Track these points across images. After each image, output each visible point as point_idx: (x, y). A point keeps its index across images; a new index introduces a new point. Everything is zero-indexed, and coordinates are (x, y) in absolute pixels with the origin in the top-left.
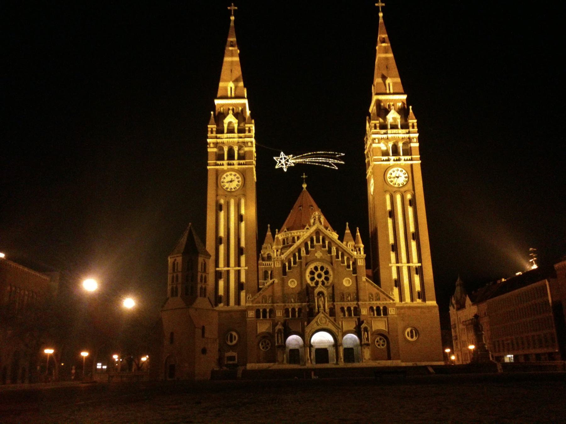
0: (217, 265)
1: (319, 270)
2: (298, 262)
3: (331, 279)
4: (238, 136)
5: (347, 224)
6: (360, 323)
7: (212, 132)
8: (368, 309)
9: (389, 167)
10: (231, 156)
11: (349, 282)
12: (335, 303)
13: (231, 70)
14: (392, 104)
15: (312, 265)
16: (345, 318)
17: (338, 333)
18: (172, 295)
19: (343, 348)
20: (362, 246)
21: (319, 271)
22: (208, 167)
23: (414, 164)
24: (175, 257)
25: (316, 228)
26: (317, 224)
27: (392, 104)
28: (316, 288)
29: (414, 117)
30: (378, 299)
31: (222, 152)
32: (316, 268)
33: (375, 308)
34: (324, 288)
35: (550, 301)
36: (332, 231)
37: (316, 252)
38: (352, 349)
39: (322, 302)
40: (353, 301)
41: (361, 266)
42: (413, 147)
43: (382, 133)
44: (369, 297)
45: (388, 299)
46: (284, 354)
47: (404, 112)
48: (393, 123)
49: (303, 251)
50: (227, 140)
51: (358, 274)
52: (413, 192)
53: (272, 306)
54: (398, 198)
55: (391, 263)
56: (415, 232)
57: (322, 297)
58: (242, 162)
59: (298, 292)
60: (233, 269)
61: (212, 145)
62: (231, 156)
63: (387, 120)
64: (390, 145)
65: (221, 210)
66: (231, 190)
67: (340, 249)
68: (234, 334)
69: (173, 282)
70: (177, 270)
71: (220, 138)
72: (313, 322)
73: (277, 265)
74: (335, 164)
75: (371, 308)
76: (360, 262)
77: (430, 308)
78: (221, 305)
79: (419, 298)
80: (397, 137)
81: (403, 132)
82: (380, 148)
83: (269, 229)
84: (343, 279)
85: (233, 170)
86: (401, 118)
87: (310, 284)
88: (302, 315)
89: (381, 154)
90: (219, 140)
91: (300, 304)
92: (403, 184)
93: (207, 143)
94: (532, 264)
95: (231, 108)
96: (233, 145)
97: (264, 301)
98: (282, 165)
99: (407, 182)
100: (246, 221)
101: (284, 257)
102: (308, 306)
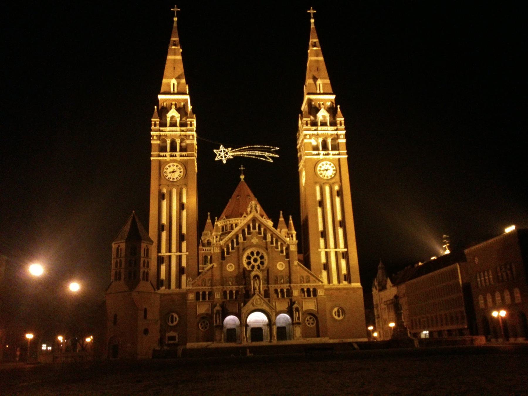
0: (159, 251)
1: (255, 255)
2: (236, 247)
3: (266, 263)
4: (180, 129)
5: (281, 212)
6: (292, 303)
7: (155, 125)
8: (300, 290)
10: (173, 148)
11: (283, 265)
12: (270, 286)
13: (174, 68)
14: (322, 103)
15: (249, 250)
16: (278, 299)
17: (272, 313)
18: (116, 280)
19: (276, 327)
20: (294, 232)
21: (255, 256)
22: (152, 158)
24: (118, 243)
25: (253, 216)
26: (254, 212)
27: (322, 103)
28: (252, 272)
29: (342, 116)
30: (308, 282)
31: (164, 144)
32: (252, 253)
33: (305, 290)
34: (259, 271)
35: (461, 283)
36: (267, 219)
37: (252, 238)
38: (284, 328)
40: (287, 283)
41: (293, 251)
42: (341, 143)
43: (313, 129)
45: (317, 281)
46: (221, 333)
47: (332, 111)
48: (322, 120)
49: (241, 238)
50: (169, 133)
51: (290, 259)
52: (340, 184)
53: (211, 289)
54: (327, 189)
55: (320, 248)
58: (184, 153)
59: (235, 275)
60: (174, 255)
61: (155, 138)
62: (173, 148)
63: (318, 118)
64: (320, 140)
65: (163, 199)
66: (173, 180)
67: (274, 235)
68: (175, 315)
69: (116, 267)
70: (121, 255)
71: (163, 131)
72: (249, 304)
73: (216, 250)
75: (302, 290)
76: (292, 247)
77: (355, 289)
78: (164, 288)
79: (345, 280)
81: (332, 129)
82: (310, 143)
83: (209, 217)
85: (175, 161)
86: (330, 116)
87: (247, 268)
88: (238, 296)
89: (312, 149)
90: (162, 133)
91: (237, 286)
93: (150, 136)
94: (445, 249)
95: (174, 103)
96: (175, 137)
97: (203, 284)
98: (222, 157)
99: (335, 174)
100: (188, 209)
101: (223, 243)
102: (245, 288)
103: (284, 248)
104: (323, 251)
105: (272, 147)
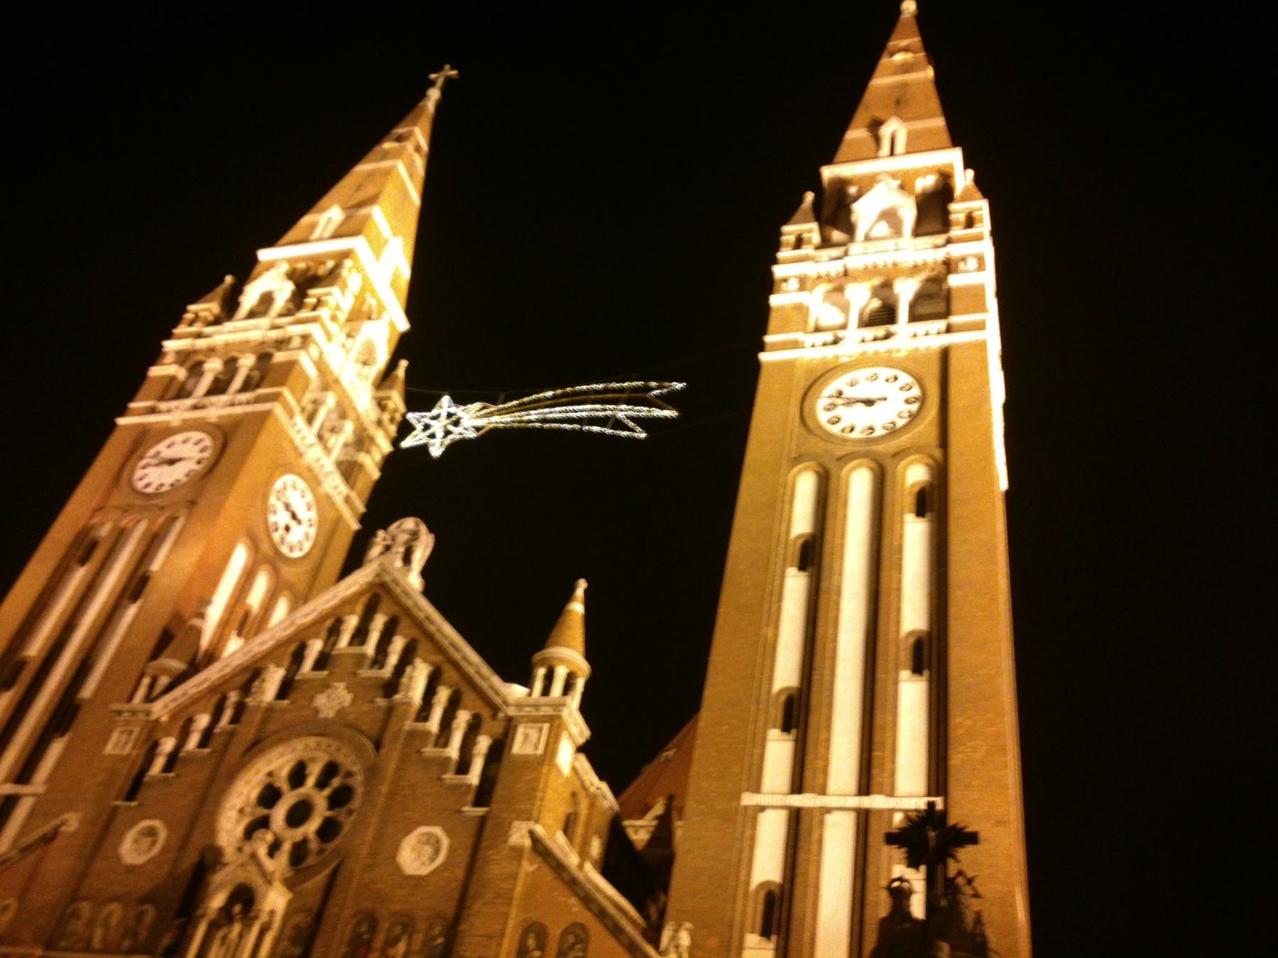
1: (311, 781)
15: (280, 749)
32: (297, 777)
37: (325, 686)
39: (223, 951)
42: (961, 289)
52: (938, 453)
64: (861, 297)
67: (449, 673)
74: (638, 420)
76: (526, 736)
84: (408, 831)
98: (432, 436)
99: (914, 417)
101: (165, 707)
103: (483, 743)
105: (653, 384)
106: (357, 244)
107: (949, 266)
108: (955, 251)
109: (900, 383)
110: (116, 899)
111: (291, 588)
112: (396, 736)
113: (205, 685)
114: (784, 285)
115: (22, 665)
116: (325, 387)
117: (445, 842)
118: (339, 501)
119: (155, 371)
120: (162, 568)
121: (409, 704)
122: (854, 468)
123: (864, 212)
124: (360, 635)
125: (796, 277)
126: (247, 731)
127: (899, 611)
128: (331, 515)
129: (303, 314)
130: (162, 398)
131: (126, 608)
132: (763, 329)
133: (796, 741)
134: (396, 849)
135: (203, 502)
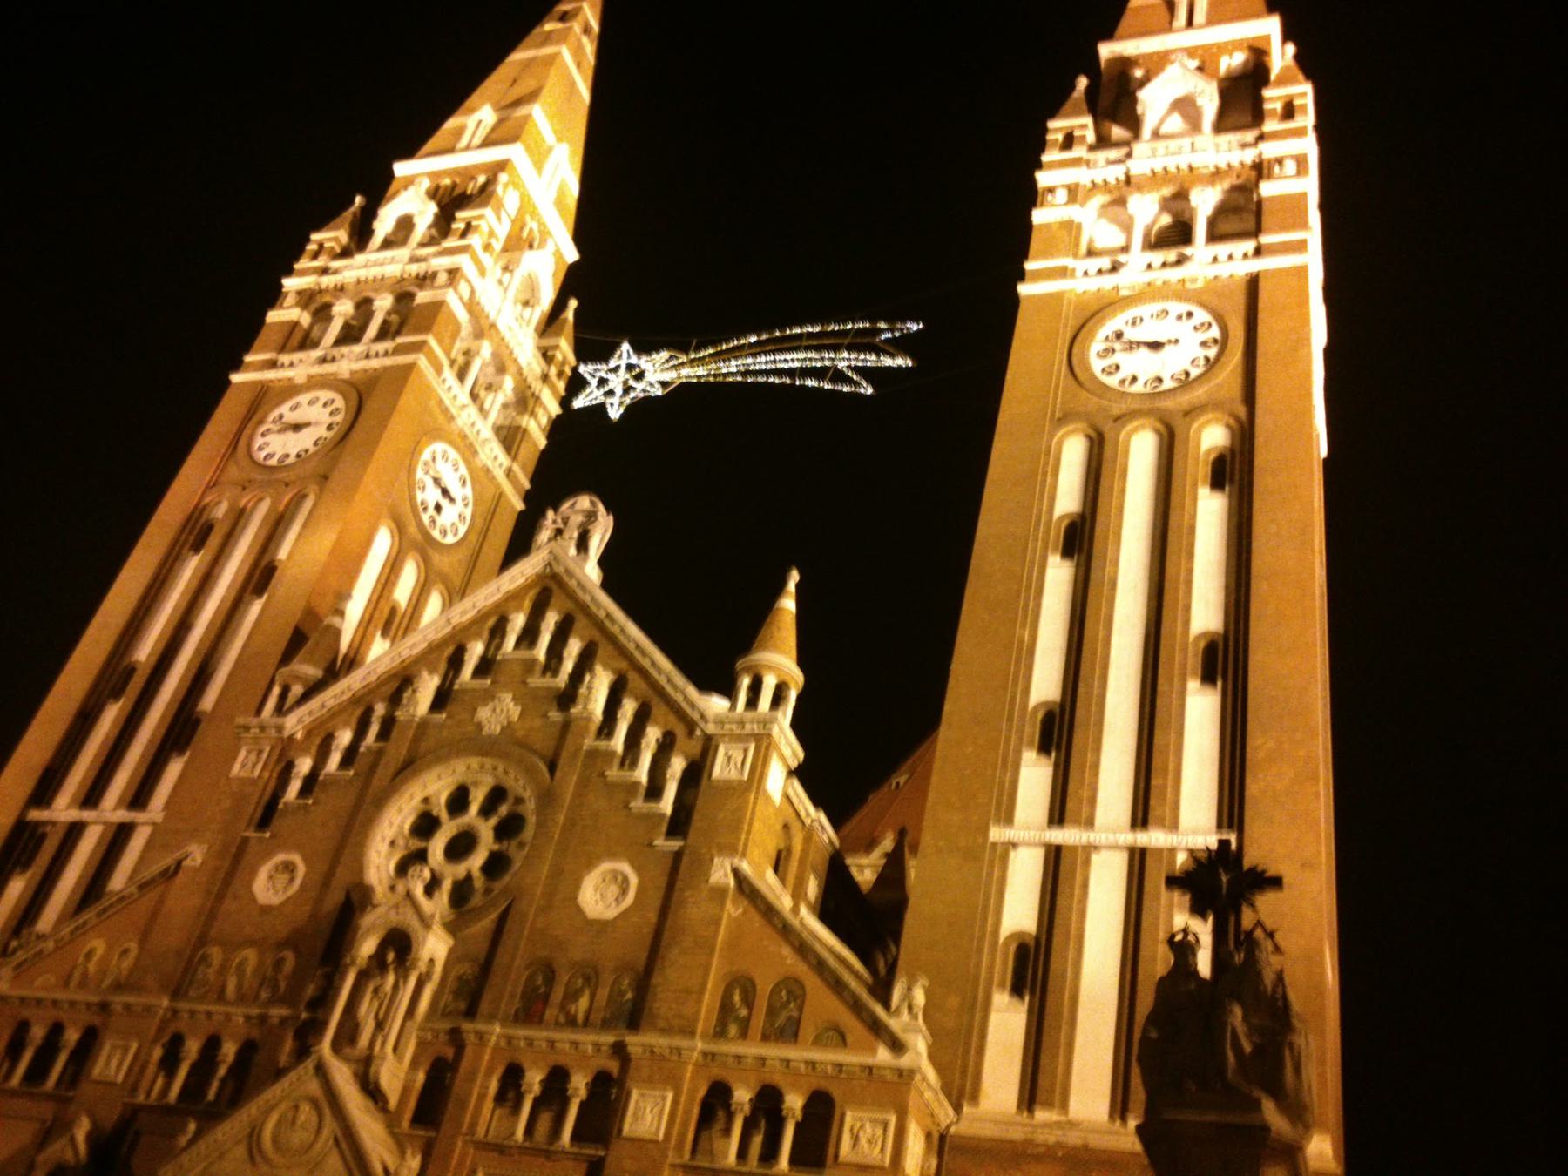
1: (474, 808)
9: (1111, 304)
23: (1266, 272)
30: (788, 1032)
32: (459, 801)
37: (488, 696)
39: (376, 1004)
40: (606, 1025)
42: (1272, 199)
44: (726, 1009)
52: (1242, 411)
56: (1226, 636)
57: (391, 967)
58: (381, 347)
64: (1147, 210)
67: (634, 680)
73: (243, 766)
74: (863, 372)
75: (717, 1099)
80: (1184, 167)
84: (590, 865)
92: (1183, 377)
98: (611, 393)
99: (1211, 364)
101: (300, 721)
103: (677, 765)
104: (1029, 844)
105: (882, 325)
106: (511, 152)
107: (1260, 170)
108: (1269, 150)
109: (1196, 321)
110: (251, 942)
111: (445, 580)
112: (575, 755)
113: (348, 695)
114: (1049, 197)
115: (131, 670)
116: (479, 334)
117: (634, 880)
118: (500, 475)
119: (273, 316)
120: (291, 555)
121: (589, 719)
122: (1136, 430)
123: (1153, 100)
124: (529, 635)
125: (1063, 186)
126: (398, 749)
127: (1188, 608)
128: (490, 492)
129: (450, 242)
130: (282, 349)
131: (250, 603)
132: (1021, 250)
133: (1056, 766)
134: (577, 886)
135: (336, 479)
